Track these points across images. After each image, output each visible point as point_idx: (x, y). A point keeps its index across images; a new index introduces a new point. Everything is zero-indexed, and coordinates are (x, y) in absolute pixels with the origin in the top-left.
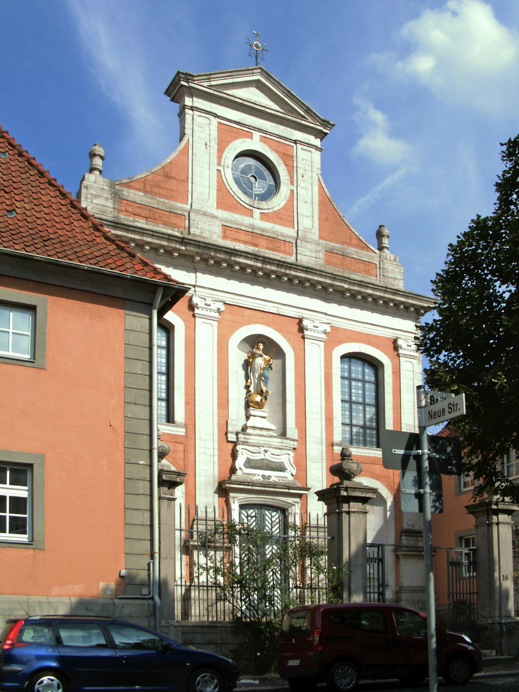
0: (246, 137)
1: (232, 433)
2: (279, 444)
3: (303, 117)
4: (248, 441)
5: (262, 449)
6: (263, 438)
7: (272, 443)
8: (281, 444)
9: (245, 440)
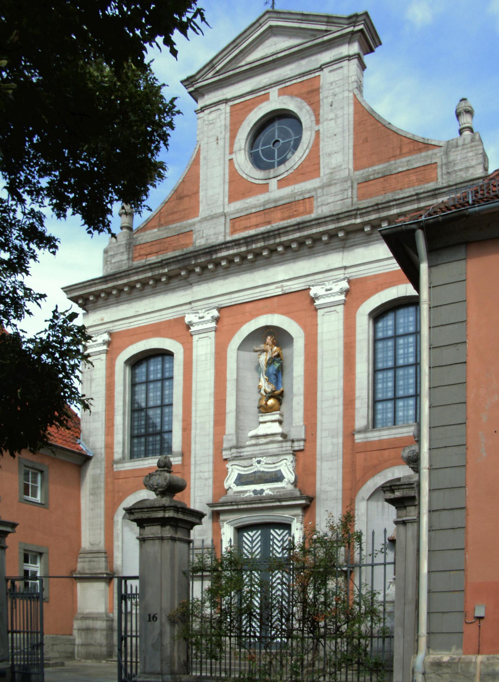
0: (262, 101)
1: (226, 449)
2: (277, 450)
3: (326, 31)
4: (242, 454)
5: (254, 460)
6: (258, 448)
7: (270, 450)
8: (281, 449)
9: (238, 455)
